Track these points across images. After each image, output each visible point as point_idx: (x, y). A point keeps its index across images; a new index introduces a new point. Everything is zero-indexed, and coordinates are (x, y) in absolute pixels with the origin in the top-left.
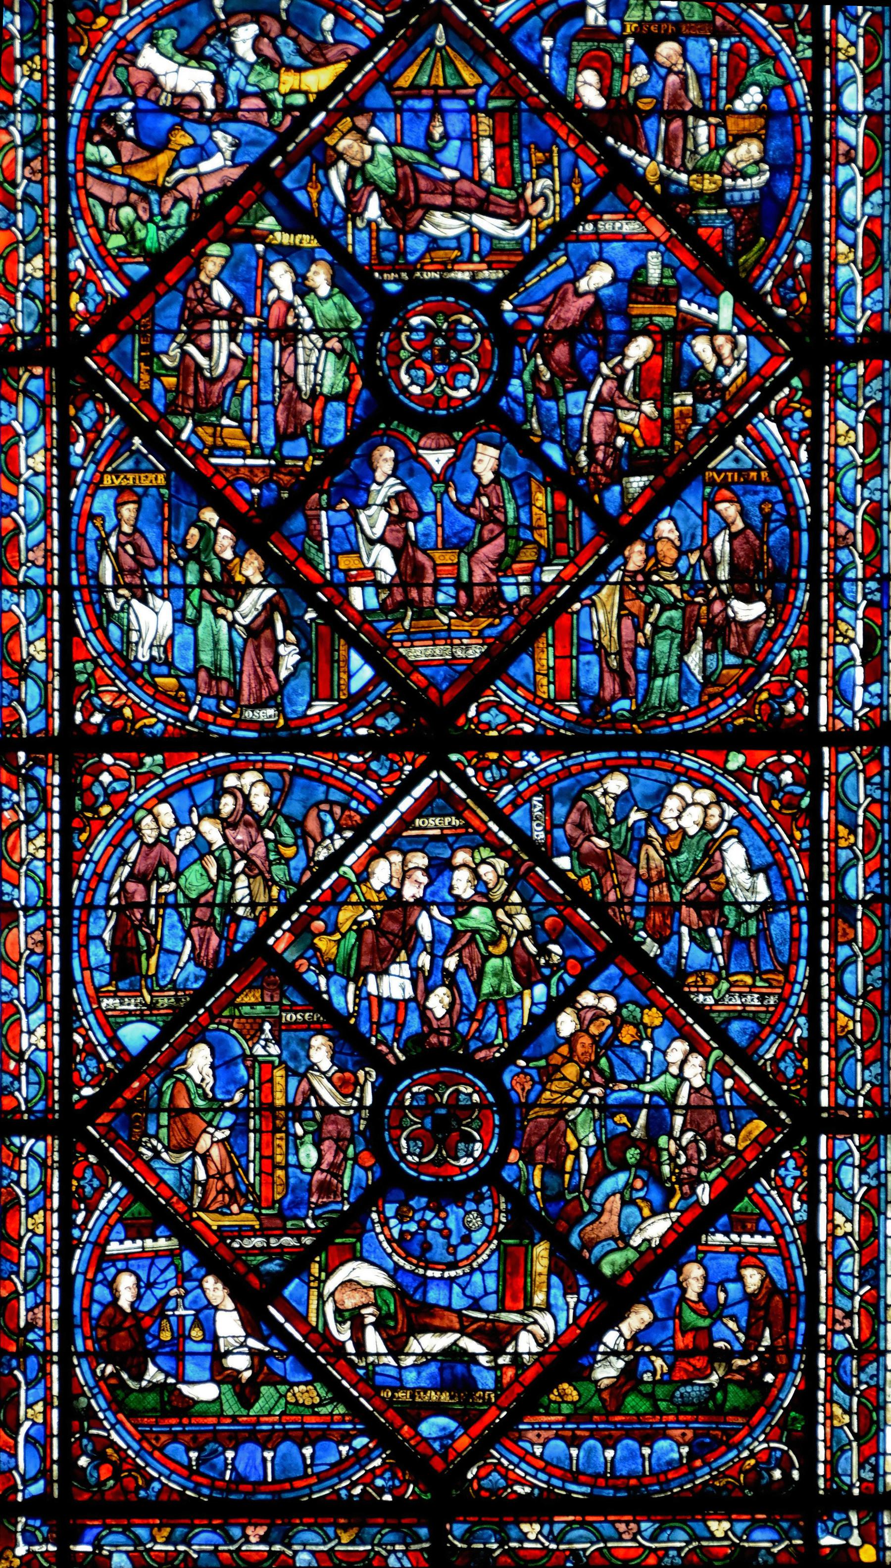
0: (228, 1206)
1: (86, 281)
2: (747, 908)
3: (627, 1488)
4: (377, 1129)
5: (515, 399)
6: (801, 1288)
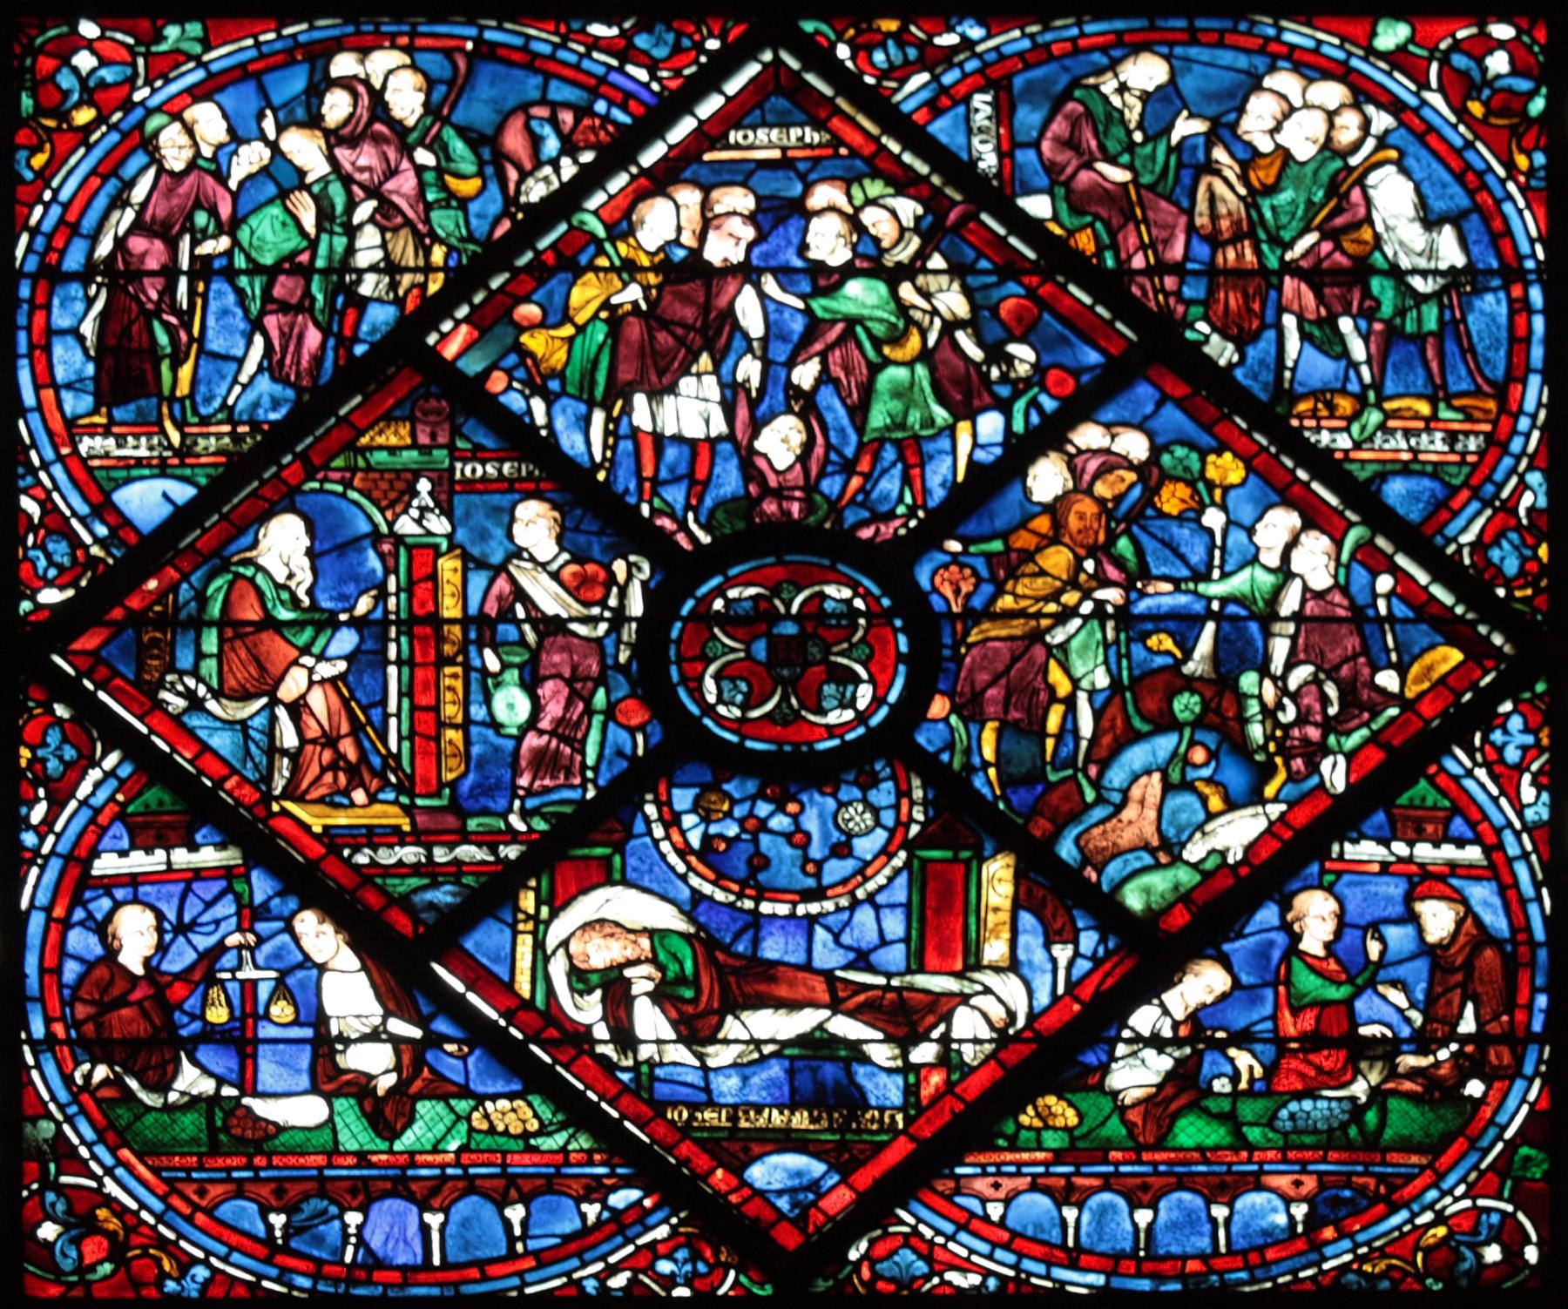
0: (346, 793)
2: (1417, 283)
3: (1182, 1276)
4: (654, 670)
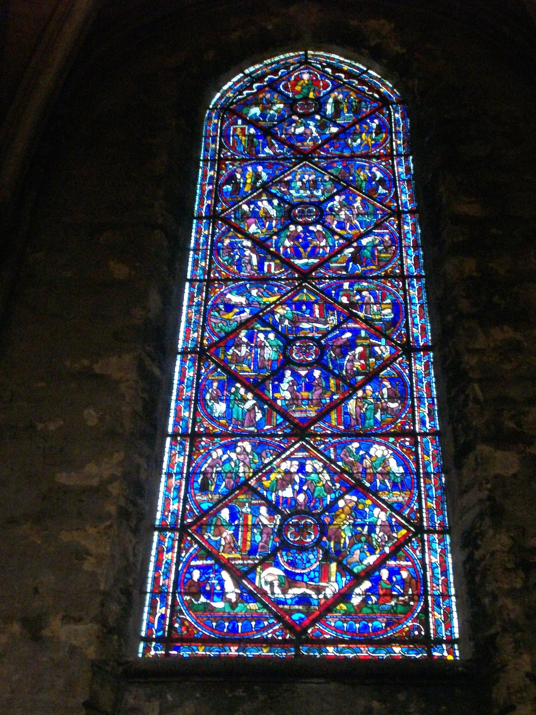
6: (421, 577)
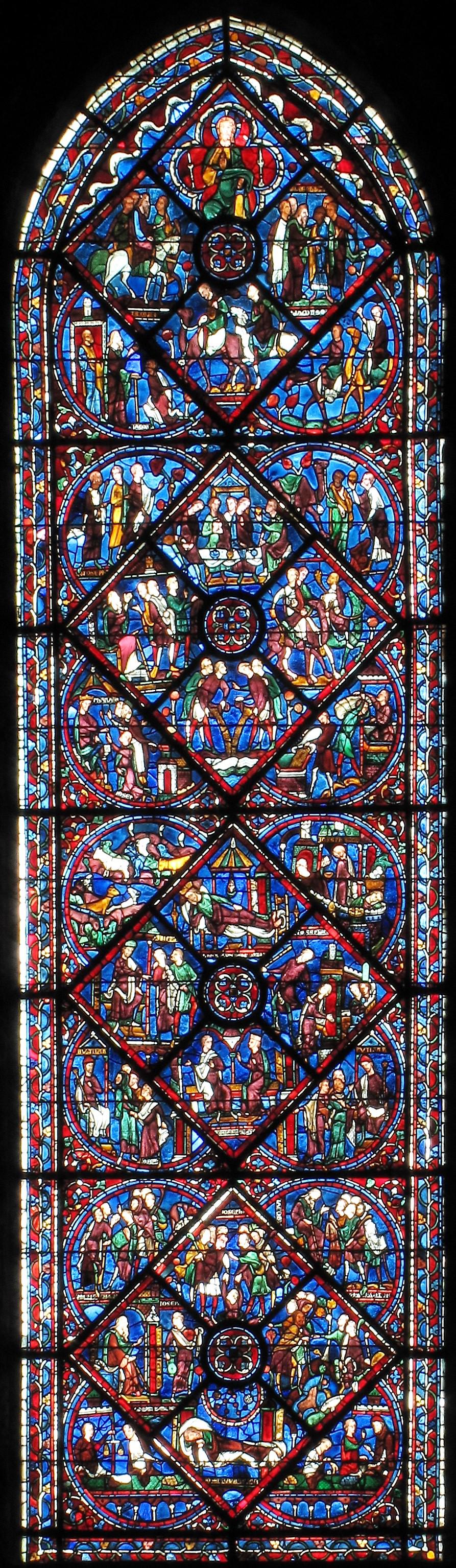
1: (70, 959)
5: (268, 1013)
